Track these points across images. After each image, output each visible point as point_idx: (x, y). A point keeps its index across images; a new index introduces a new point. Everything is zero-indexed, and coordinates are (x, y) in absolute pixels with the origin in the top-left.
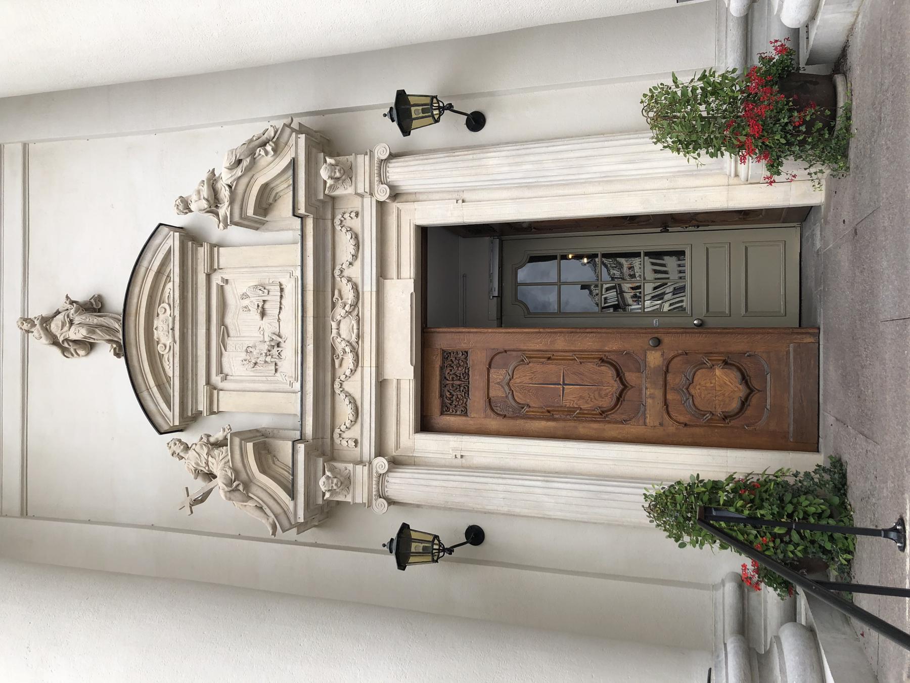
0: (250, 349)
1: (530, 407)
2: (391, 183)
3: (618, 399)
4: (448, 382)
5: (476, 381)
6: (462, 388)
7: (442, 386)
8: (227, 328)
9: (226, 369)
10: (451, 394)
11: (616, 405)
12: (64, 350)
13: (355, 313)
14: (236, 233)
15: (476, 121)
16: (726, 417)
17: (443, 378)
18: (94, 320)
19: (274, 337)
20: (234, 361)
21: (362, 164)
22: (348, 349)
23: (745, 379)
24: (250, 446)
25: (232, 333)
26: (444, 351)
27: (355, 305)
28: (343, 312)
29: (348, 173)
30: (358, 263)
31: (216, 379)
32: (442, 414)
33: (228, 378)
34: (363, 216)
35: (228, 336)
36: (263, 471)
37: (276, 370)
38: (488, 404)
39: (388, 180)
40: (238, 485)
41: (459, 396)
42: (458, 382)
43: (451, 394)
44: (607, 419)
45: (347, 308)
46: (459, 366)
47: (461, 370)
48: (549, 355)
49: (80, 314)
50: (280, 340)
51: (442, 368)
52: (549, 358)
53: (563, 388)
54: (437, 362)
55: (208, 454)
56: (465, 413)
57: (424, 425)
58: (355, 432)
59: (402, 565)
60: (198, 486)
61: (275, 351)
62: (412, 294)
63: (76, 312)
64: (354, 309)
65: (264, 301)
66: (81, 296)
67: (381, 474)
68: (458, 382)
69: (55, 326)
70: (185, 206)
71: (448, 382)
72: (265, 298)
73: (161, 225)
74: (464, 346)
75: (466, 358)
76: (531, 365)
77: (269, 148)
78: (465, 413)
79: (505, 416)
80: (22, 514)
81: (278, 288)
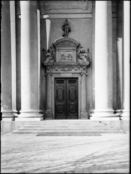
18: (68, 31)
20: (62, 53)
21: (85, 71)
29: (84, 69)
30: (74, 70)
54: (63, 79)
57: (55, 78)
58: (54, 70)
66: (72, 29)
74: (65, 83)
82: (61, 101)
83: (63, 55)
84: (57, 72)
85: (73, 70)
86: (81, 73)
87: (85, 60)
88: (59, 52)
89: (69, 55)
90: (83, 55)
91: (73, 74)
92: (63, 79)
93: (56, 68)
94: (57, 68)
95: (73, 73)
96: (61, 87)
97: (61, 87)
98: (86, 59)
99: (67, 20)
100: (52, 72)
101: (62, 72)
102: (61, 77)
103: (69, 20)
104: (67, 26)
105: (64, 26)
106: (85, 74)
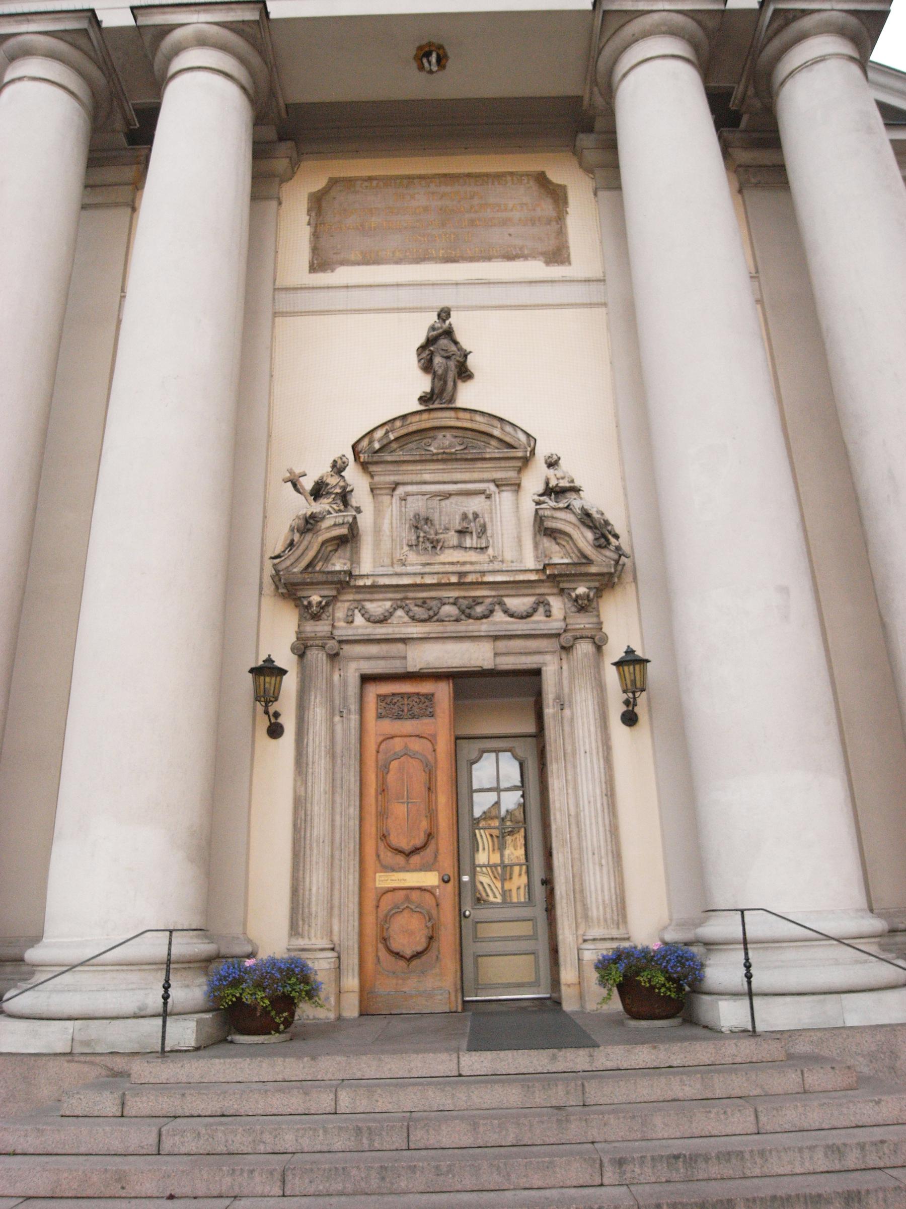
0: (429, 523)
1: (387, 774)
2: (574, 647)
3: (396, 850)
4: (406, 700)
5: (408, 726)
6: (401, 713)
7: (402, 695)
8: (448, 498)
9: (409, 499)
10: (396, 703)
11: (393, 849)
12: (422, 348)
13: (463, 617)
14: (528, 508)
15: (630, 719)
16: (385, 940)
17: (409, 695)
18: (451, 375)
19: (440, 544)
22: (431, 613)
23: (418, 955)
24: (344, 531)
25: (443, 503)
26: (433, 695)
27: (469, 617)
28: (464, 607)
31: (401, 490)
32: (378, 696)
33: (404, 502)
34: (545, 622)
35: (440, 500)
36: (323, 543)
37: (411, 546)
38: (387, 736)
39: (578, 645)
40: (311, 524)
41: (393, 711)
42: (406, 710)
43: (396, 703)
44: (379, 840)
45: (467, 611)
46: (420, 709)
47: (416, 710)
48: (433, 788)
49: (456, 366)
50: (439, 548)
51: (418, 694)
52: (429, 789)
53: (403, 803)
55: (337, 493)
56: (380, 716)
59: (252, 671)
60: (308, 484)
61: (429, 545)
62: (481, 667)
63: (458, 361)
64: (467, 616)
65: (471, 533)
66: (471, 362)
67: (324, 647)
68: (406, 710)
69: (444, 342)
70: (552, 464)
71: (406, 700)
72: (474, 534)
73: (535, 440)
74: (438, 712)
75: (427, 716)
76: (424, 773)
77: (603, 540)
78: (380, 716)
79: (378, 752)
80: (275, 313)
81: (483, 545)
82: (415, 859)
83: (427, 520)
84: (381, 631)
85: (499, 616)
86: (558, 635)
87: (584, 538)
88: (396, 500)
89: (465, 517)
90: (568, 507)
91: (502, 645)
92: (425, 688)
93: (369, 606)
94: (376, 608)
95: (496, 638)
96: (416, 745)
97: (416, 745)
98: (590, 535)
99: (444, 314)
100: (343, 631)
101: (416, 630)
102: (411, 669)
103: (455, 320)
104: (444, 342)
105: (430, 341)
106: (592, 638)
